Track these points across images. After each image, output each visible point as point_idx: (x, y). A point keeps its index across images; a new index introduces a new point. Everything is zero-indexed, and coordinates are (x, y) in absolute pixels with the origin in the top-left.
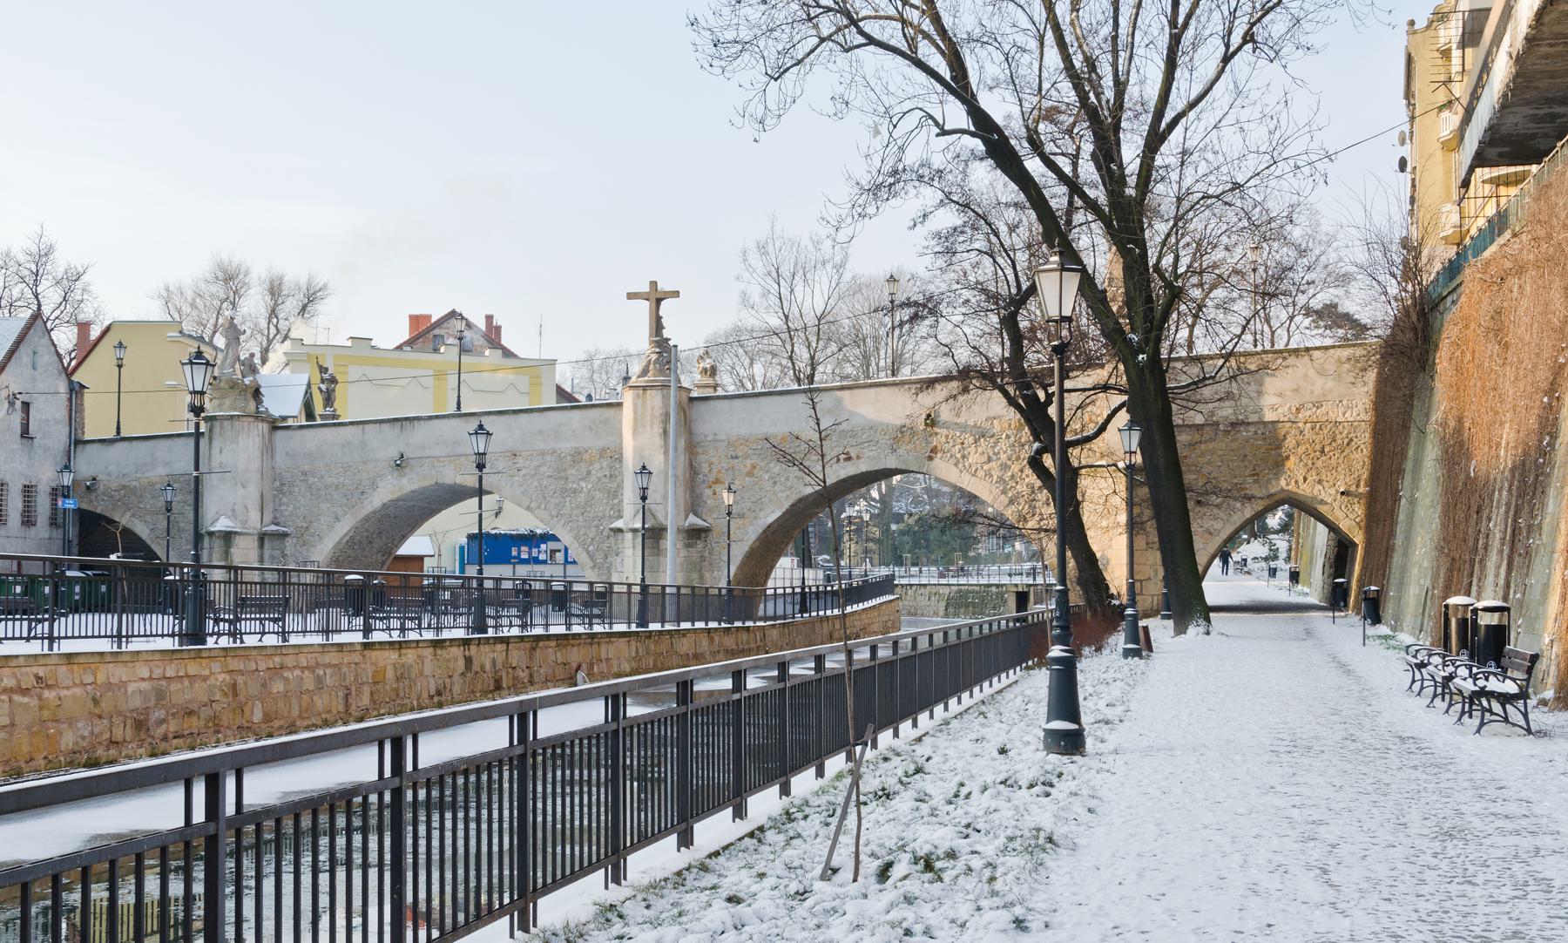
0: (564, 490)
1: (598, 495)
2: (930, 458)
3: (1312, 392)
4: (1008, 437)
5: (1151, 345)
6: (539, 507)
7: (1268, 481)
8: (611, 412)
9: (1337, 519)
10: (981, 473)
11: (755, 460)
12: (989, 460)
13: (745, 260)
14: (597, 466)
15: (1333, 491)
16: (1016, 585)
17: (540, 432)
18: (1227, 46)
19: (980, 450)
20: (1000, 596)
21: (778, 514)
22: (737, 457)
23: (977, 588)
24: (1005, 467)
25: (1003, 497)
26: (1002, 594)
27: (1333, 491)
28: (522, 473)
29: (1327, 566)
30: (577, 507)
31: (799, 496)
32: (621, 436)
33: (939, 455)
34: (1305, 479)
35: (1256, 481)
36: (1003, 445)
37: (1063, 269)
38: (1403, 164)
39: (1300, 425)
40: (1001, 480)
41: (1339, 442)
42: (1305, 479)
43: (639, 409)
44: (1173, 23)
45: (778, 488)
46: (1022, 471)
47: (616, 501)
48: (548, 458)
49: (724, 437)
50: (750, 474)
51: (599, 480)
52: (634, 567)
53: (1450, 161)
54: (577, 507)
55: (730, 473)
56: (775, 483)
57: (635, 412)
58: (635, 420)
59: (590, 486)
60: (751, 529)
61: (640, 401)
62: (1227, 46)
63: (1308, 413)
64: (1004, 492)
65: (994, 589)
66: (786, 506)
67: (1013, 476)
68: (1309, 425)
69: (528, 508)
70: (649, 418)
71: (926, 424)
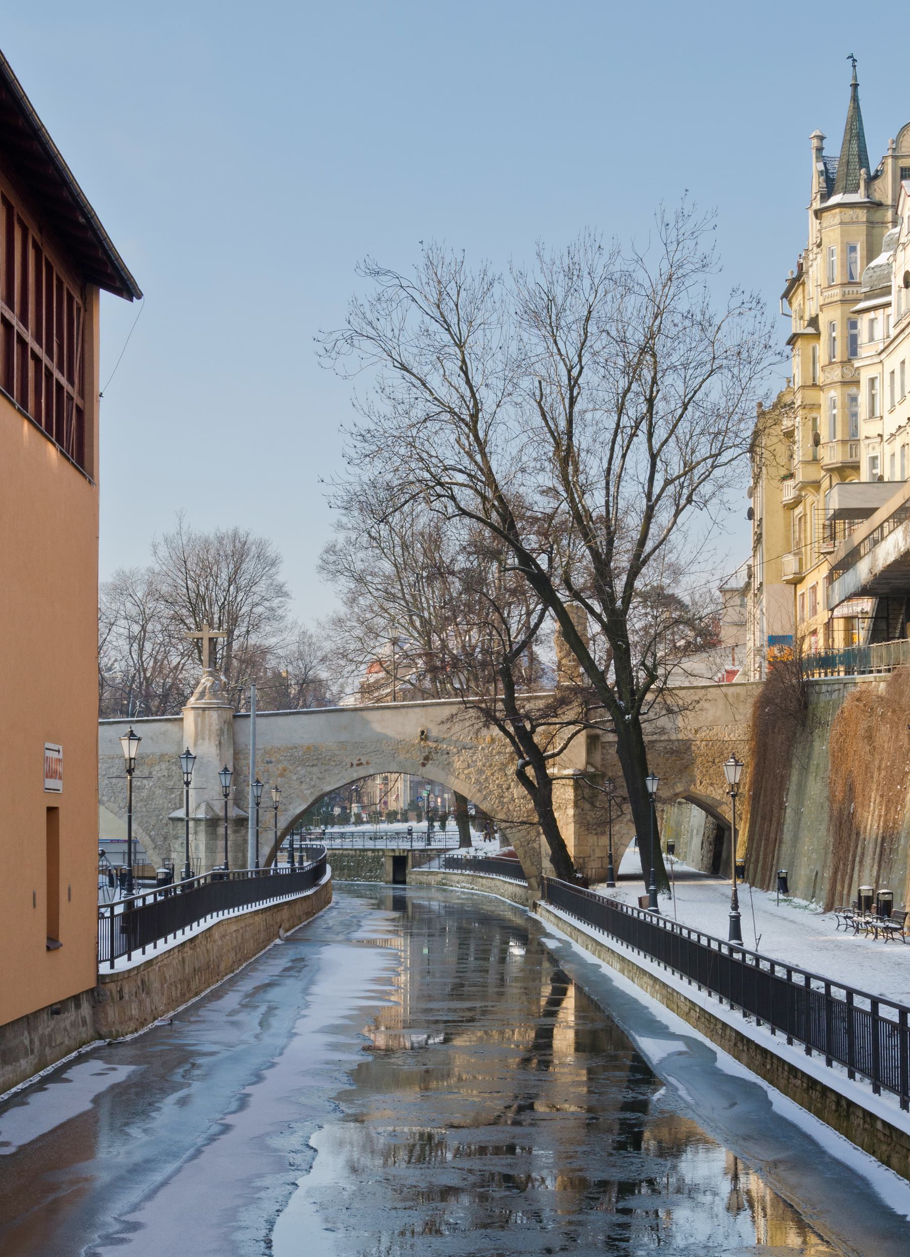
1: (159, 791)
2: (424, 765)
3: (707, 718)
4: (483, 749)
5: (635, 710)
6: (109, 801)
7: (675, 784)
9: (725, 812)
10: (462, 776)
12: (469, 766)
13: (155, 553)
14: (157, 768)
15: (720, 791)
16: (393, 850)
17: (110, 741)
18: (678, 505)
19: (461, 758)
20: (377, 860)
21: (304, 807)
22: (271, 762)
23: (351, 852)
24: (480, 772)
25: (478, 795)
26: (379, 858)
27: (720, 791)
29: (706, 844)
30: (141, 800)
31: (321, 793)
33: (430, 762)
34: (701, 783)
35: (665, 784)
36: (479, 755)
37: (736, 765)
38: (751, 514)
39: (698, 742)
40: (478, 781)
41: (726, 755)
42: (701, 783)
43: (200, 725)
44: (649, 496)
45: (304, 786)
46: (493, 774)
47: (173, 796)
48: (117, 761)
49: (261, 747)
50: (281, 775)
51: (159, 778)
53: (789, 518)
54: (141, 800)
55: (266, 774)
56: (301, 782)
59: (151, 784)
61: (199, 720)
62: (678, 505)
63: (703, 734)
64: (479, 791)
65: (370, 854)
66: (311, 800)
67: (487, 778)
68: (704, 743)
70: (207, 732)
71: (422, 739)
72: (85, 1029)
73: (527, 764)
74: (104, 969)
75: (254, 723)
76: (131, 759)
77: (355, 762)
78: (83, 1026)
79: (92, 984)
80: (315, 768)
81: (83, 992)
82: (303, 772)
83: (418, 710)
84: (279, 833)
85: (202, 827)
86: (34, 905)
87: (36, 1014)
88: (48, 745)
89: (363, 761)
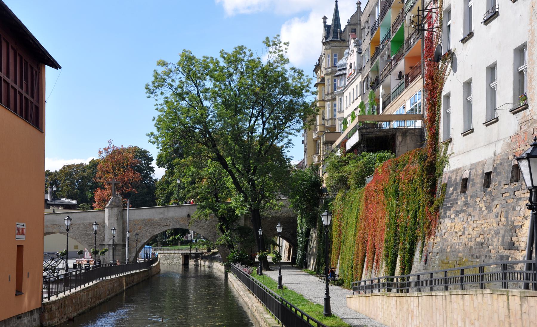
0: (85, 234)
2: (188, 225)
8: (100, 213)
11: (141, 225)
17: (79, 218)
21: (147, 240)
28: (74, 229)
32: (104, 219)
45: (147, 233)
48: (81, 225)
50: (139, 229)
52: (109, 254)
57: (109, 213)
58: (109, 216)
60: (140, 244)
61: (110, 211)
65: (176, 255)
69: (75, 239)
72: (35, 322)
73: (222, 225)
74: (46, 301)
75: (129, 212)
76: (68, 226)
77: (165, 225)
78: (34, 321)
79: (40, 306)
80: (151, 227)
81: (35, 309)
82: (147, 228)
83: (187, 207)
84: (138, 249)
85: (111, 247)
86: (9, 280)
87: (10, 319)
88: (17, 223)
89: (168, 224)
